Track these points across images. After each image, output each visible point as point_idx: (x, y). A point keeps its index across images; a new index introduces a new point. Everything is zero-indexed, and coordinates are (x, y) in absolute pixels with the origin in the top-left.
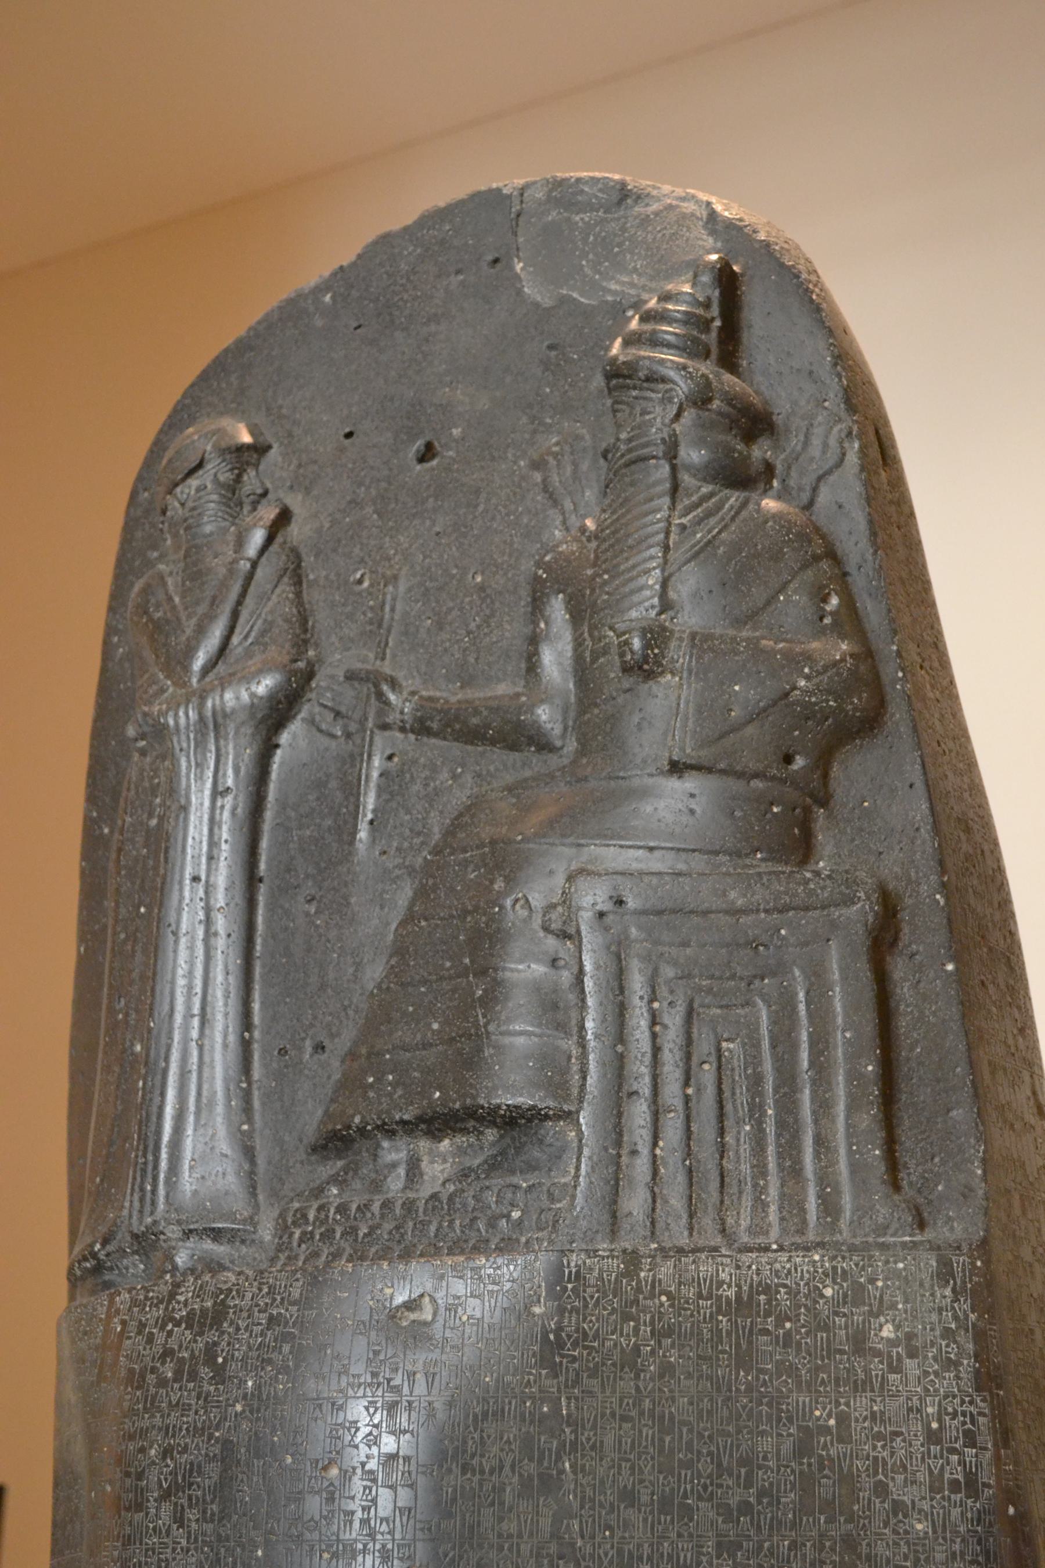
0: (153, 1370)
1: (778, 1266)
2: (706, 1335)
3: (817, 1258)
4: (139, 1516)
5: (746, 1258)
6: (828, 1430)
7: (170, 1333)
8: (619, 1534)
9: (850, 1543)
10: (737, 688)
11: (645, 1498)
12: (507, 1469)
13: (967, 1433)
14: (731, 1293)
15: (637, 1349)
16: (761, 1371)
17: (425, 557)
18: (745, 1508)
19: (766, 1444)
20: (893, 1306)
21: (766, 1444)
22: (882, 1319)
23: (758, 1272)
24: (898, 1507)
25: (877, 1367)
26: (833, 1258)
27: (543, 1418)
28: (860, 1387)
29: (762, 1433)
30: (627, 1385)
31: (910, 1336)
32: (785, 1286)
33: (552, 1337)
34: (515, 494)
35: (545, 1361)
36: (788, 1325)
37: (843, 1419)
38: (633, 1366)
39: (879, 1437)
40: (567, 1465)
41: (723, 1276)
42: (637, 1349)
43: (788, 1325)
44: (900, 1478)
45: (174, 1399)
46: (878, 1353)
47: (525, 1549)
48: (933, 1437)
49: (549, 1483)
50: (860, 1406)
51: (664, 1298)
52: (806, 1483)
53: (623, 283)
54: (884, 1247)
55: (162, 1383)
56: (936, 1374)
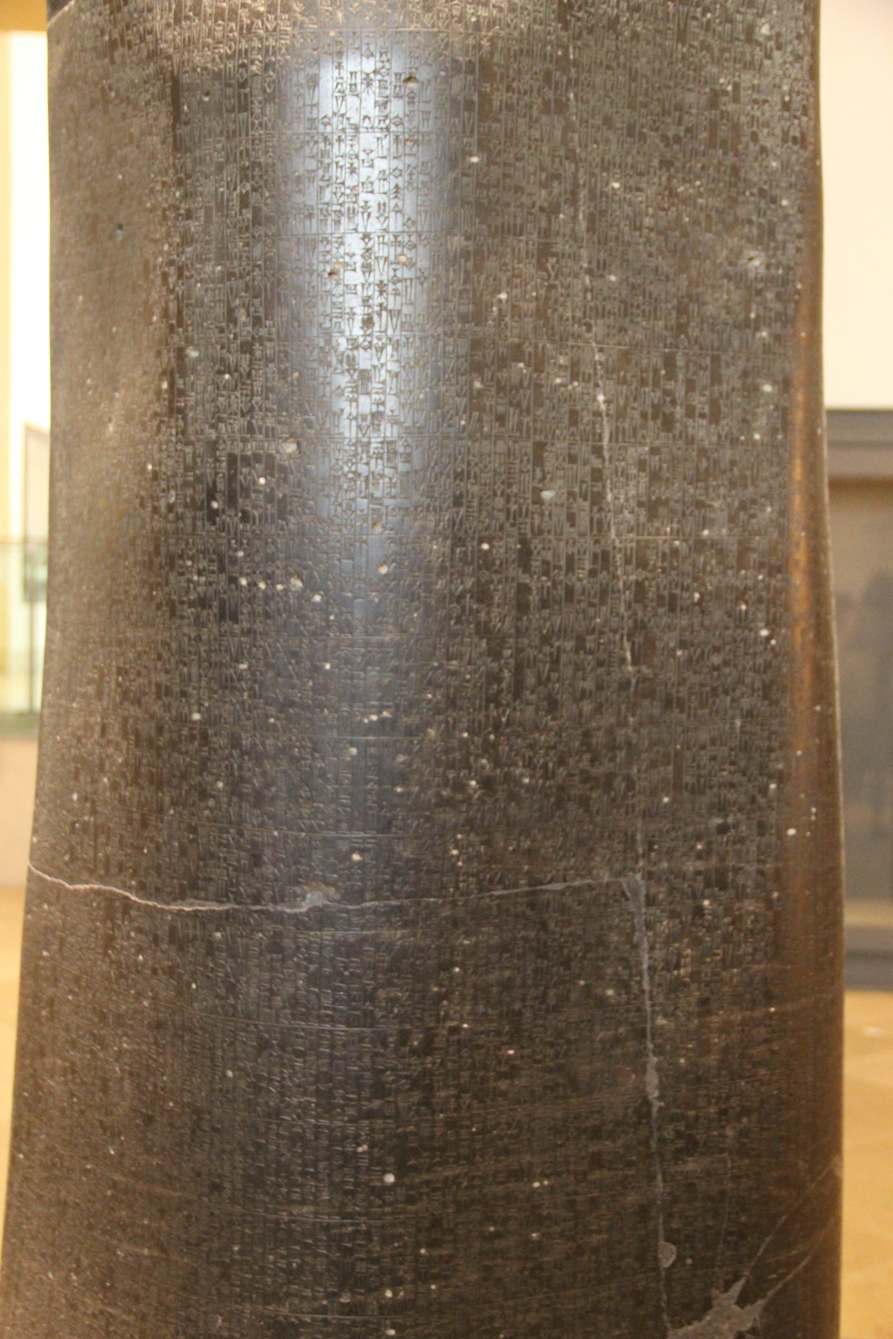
2: (660, 15)
4: (243, 116)
6: (725, 93)
8: (602, 147)
9: (735, 170)
11: (618, 125)
12: (535, 93)
13: (804, 107)
15: (617, 17)
16: (691, 46)
18: (677, 139)
19: (691, 98)
21: (691, 98)
24: (763, 150)
27: (559, 59)
28: (748, 65)
29: (689, 90)
30: (610, 43)
35: (561, 19)
38: (615, 30)
39: (755, 101)
40: (572, 96)
42: (617, 17)
44: (765, 131)
45: (270, 27)
47: (545, 149)
48: (786, 106)
49: (561, 107)
50: (747, 78)
52: (713, 126)
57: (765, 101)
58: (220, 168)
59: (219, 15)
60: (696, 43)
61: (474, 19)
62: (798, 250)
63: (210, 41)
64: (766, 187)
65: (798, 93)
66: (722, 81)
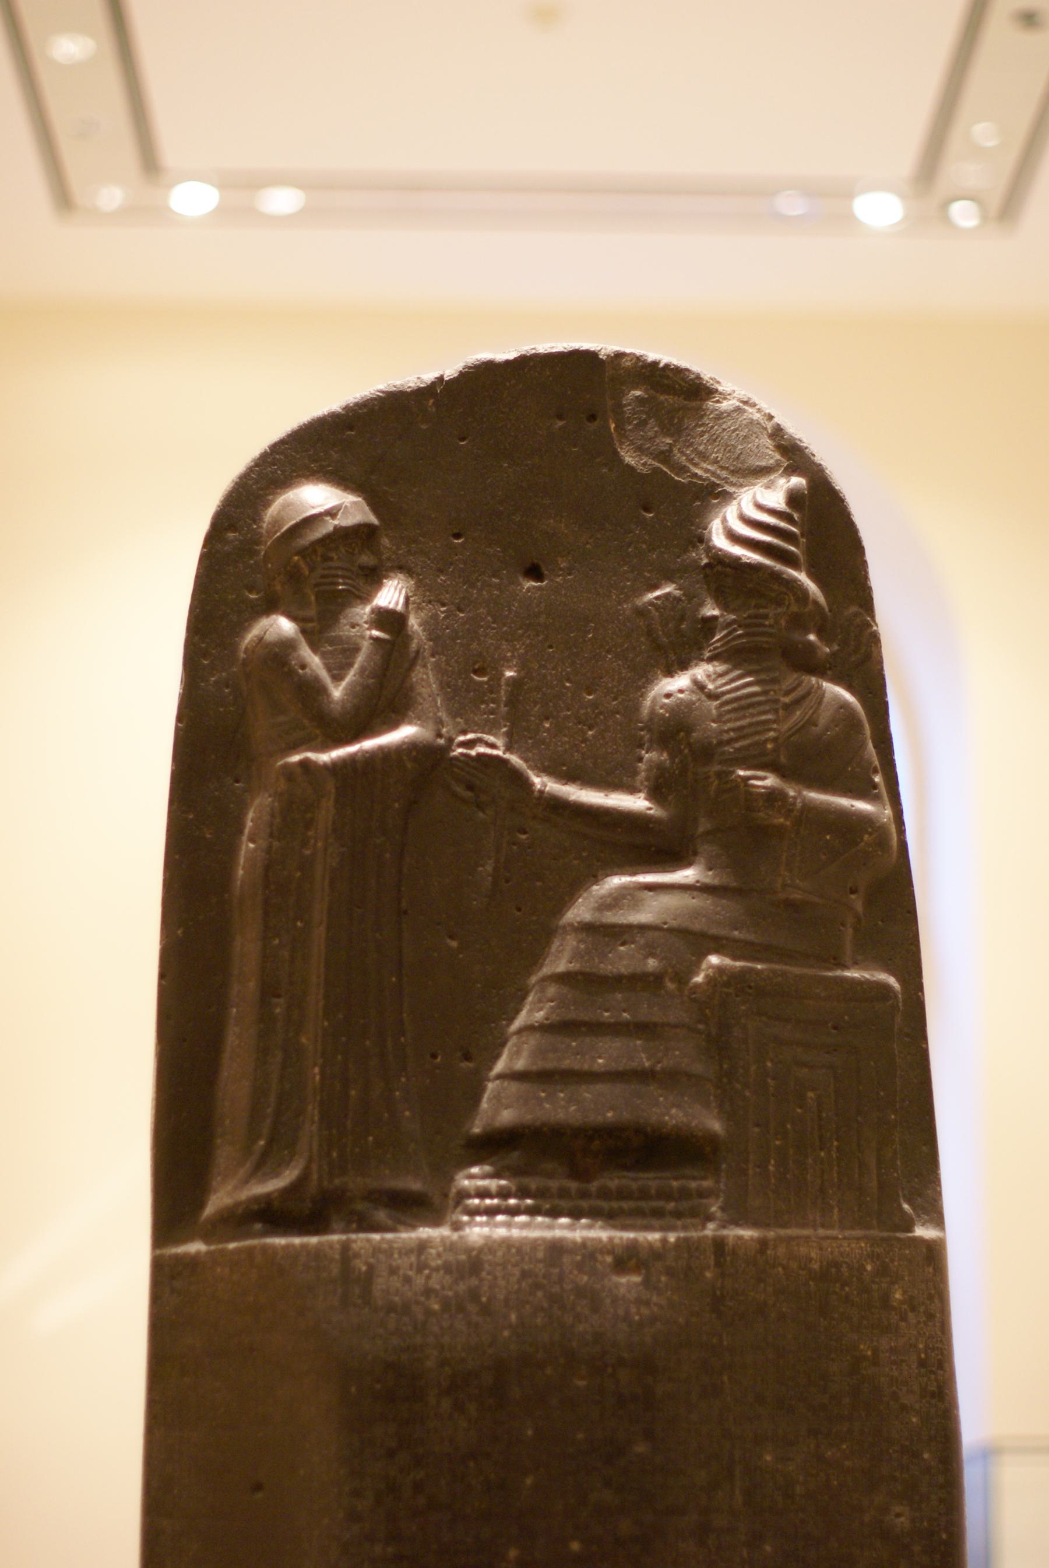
0: (417, 1303)
1: (842, 1249)
3: (863, 1245)
5: (825, 1244)
7: (428, 1277)
10: (828, 837)
14: (816, 1266)
17: (541, 666)
20: (903, 1279)
22: (897, 1286)
23: (832, 1253)
24: (904, 1408)
25: (894, 1318)
26: (872, 1246)
31: (912, 1298)
32: (846, 1263)
33: (718, 1293)
34: (620, 630)
36: (847, 1289)
37: (876, 1351)
39: (894, 1363)
40: (725, 1378)
41: (813, 1255)
43: (847, 1289)
44: (905, 1389)
45: (445, 1324)
46: (894, 1308)
48: (922, 1364)
51: (780, 1269)
53: (707, 471)
54: (899, 1239)
55: (429, 1313)
56: (925, 1323)
57: (902, 1361)
58: (391, 1454)
59: (391, 1308)
60: (836, 1316)
61: (637, 1318)
62: (941, 1500)
63: (381, 1331)
64: (907, 1443)
65: (933, 1349)
66: (862, 1347)
